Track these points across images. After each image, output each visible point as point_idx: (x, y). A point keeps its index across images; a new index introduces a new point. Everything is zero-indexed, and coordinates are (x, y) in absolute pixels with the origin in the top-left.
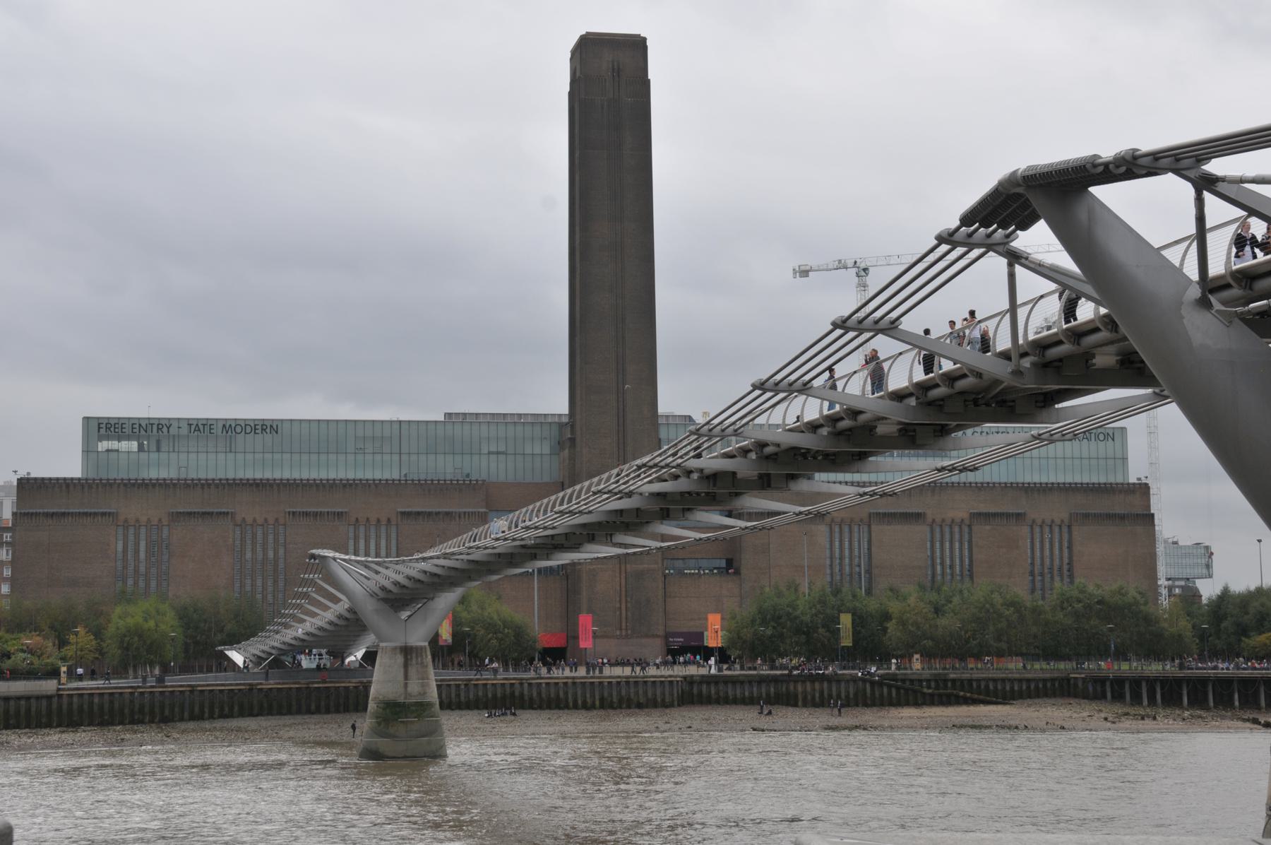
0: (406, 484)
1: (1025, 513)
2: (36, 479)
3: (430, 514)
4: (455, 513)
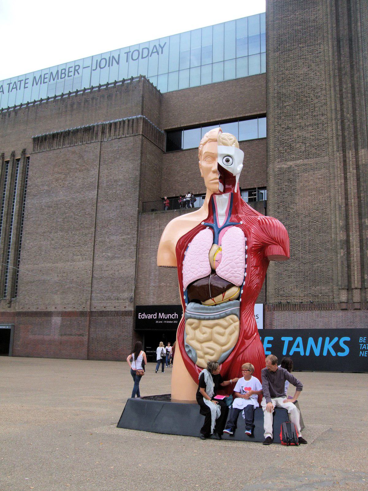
3: (66, 134)
4: (98, 126)
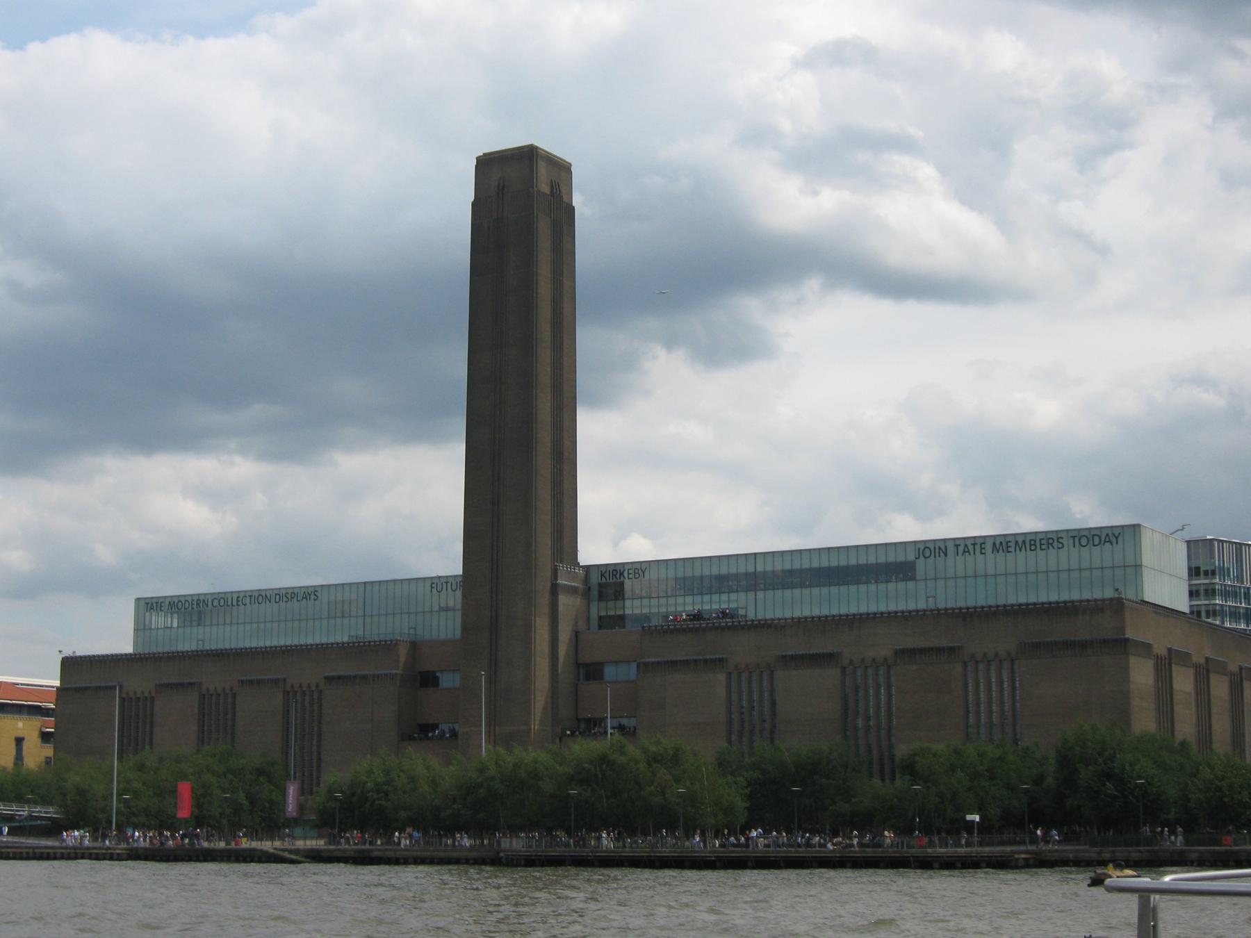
0: (332, 647)
1: (959, 648)
2: (76, 658)
3: (348, 677)
4: (370, 675)
